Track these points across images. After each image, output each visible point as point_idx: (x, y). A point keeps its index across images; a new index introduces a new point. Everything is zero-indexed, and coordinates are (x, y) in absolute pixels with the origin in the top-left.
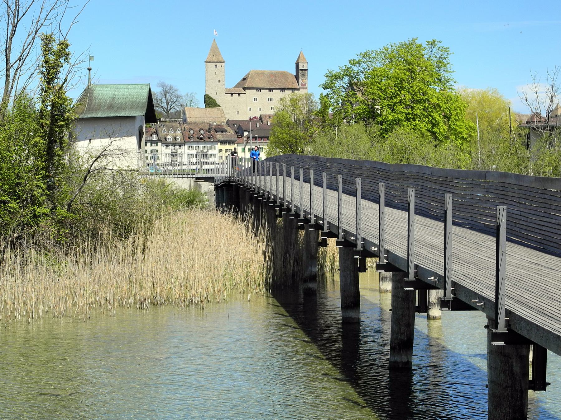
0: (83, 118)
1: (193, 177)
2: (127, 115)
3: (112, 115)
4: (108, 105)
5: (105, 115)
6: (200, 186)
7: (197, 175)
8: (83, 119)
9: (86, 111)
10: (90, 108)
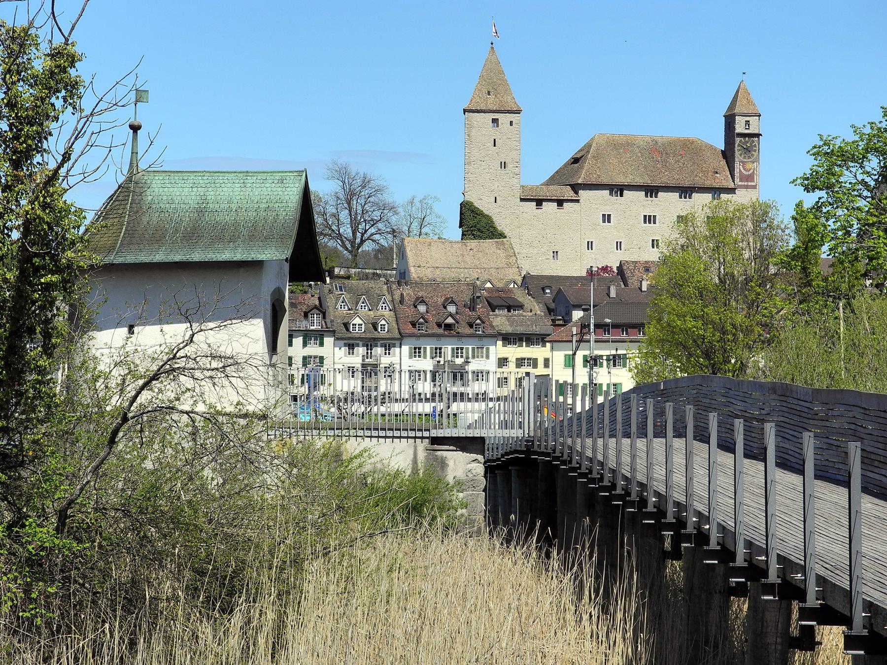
0: (113, 264)
1: (422, 438)
2: (239, 256)
3: (197, 256)
5: (177, 258)
6: (443, 464)
7: (434, 431)
8: (110, 269)
9: (122, 244)
10: (133, 237)
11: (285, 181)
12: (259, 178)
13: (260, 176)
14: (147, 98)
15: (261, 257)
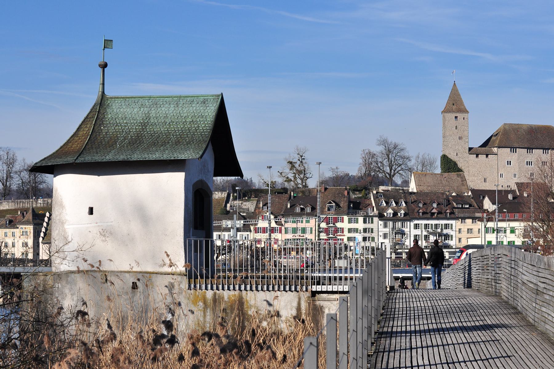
2: (166, 156)
3: (136, 156)
4: (131, 137)
5: (121, 158)
11: (206, 102)
12: (188, 100)
13: (189, 99)
14: (112, 45)
15: (182, 157)
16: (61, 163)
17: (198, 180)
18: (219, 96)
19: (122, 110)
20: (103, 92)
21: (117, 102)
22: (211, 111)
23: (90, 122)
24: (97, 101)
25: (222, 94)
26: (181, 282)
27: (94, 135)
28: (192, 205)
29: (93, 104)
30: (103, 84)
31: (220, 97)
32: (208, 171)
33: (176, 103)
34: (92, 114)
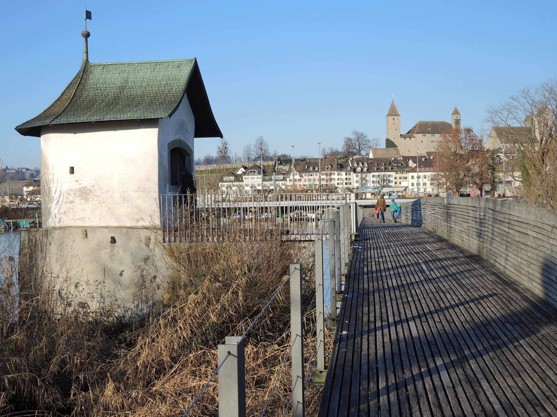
3: (107, 118)
4: (109, 99)
11: (181, 67)
16: (39, 125)
17: (175, 139)
18: (192, 60)
19: (103, 76)
20: (87, 60)
21: (99, 68)
22: (185, 73)
23: (73, 87)
24: (81, 68)
25: (196, 59)
26: (150, 239)
27: (75, 98)
28: (167, 162)
29: (78, 71)
30: (87, 52)
31: (194, 61)
32: (187, 131)
33: (153, 68)
34: (75, 80)
